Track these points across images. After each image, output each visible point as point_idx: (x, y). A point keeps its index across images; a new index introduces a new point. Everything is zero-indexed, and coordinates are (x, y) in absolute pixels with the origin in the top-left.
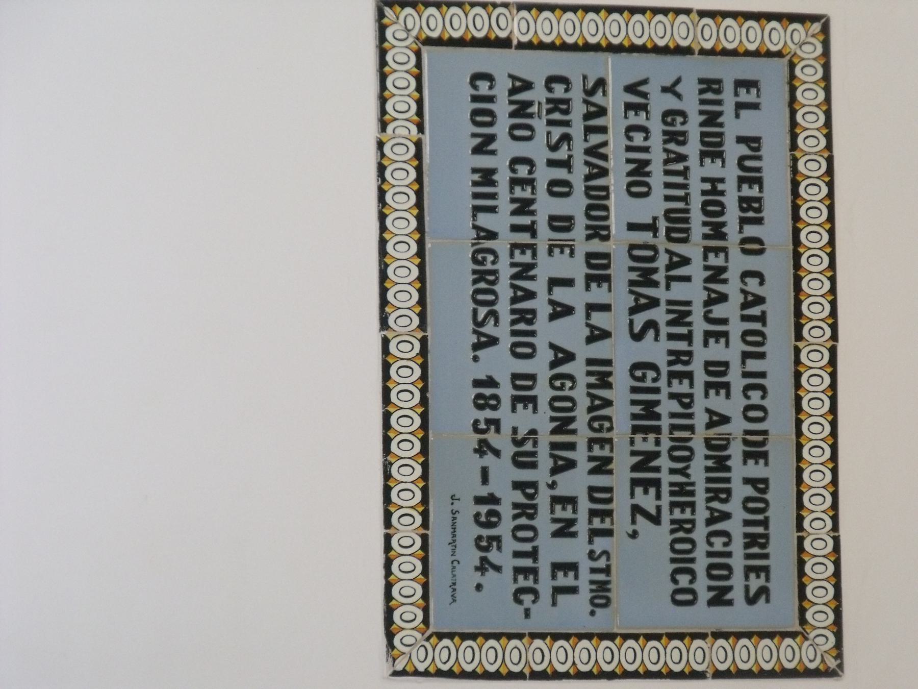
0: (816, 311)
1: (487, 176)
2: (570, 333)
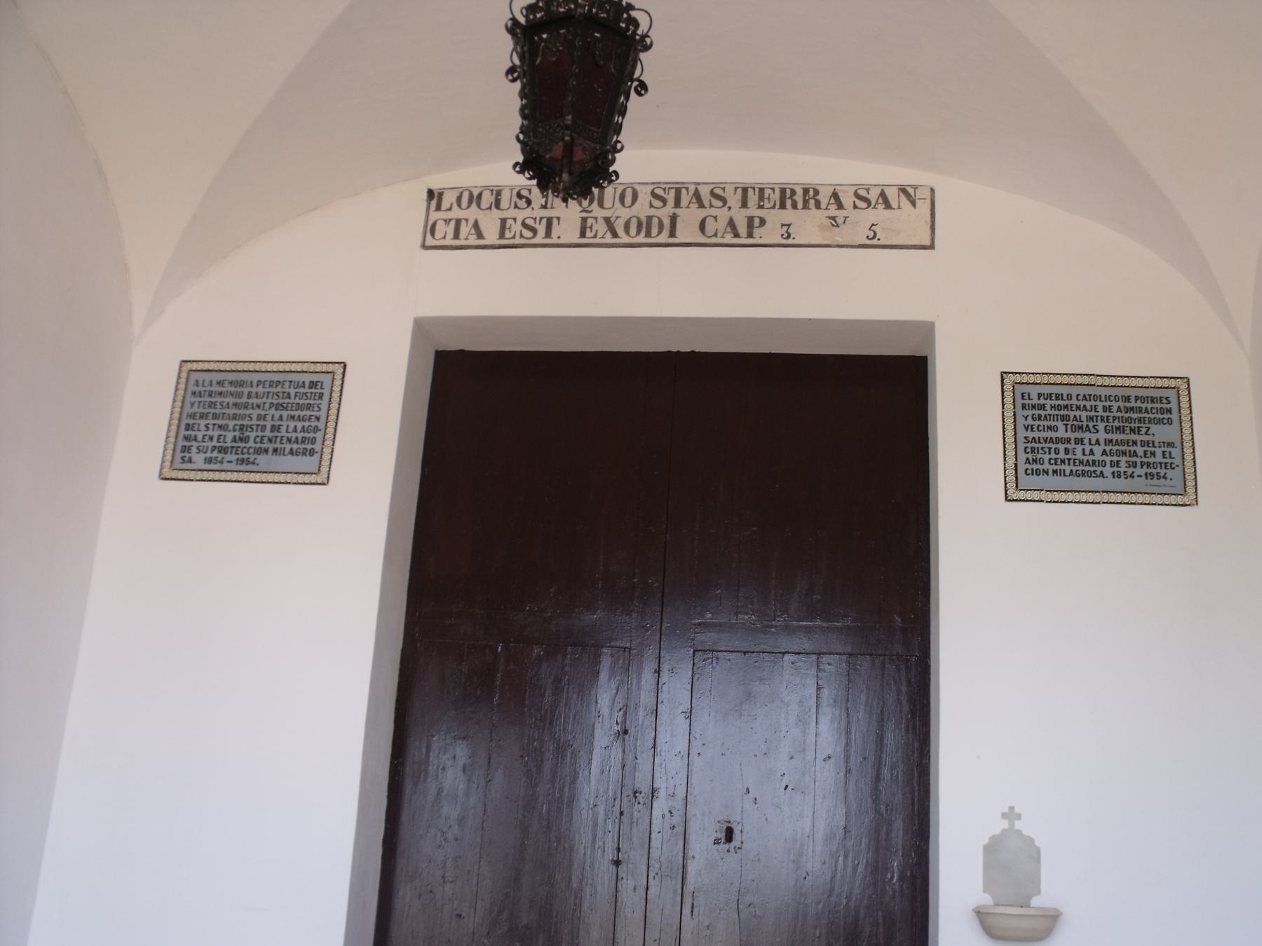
0: (1086, 380)
1: (1055, 472)
2: (1098, 450)
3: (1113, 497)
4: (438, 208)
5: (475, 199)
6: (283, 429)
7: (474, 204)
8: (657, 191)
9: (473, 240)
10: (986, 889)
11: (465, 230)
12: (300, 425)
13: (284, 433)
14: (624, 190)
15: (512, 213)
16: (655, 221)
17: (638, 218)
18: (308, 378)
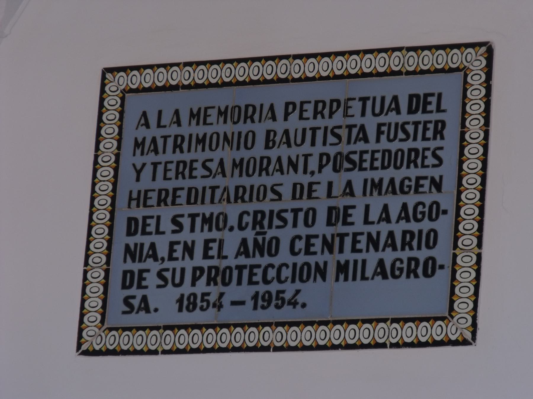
6: (357, 216)
12: (395, 204)
13: (359, 226)
18: (404, 88)
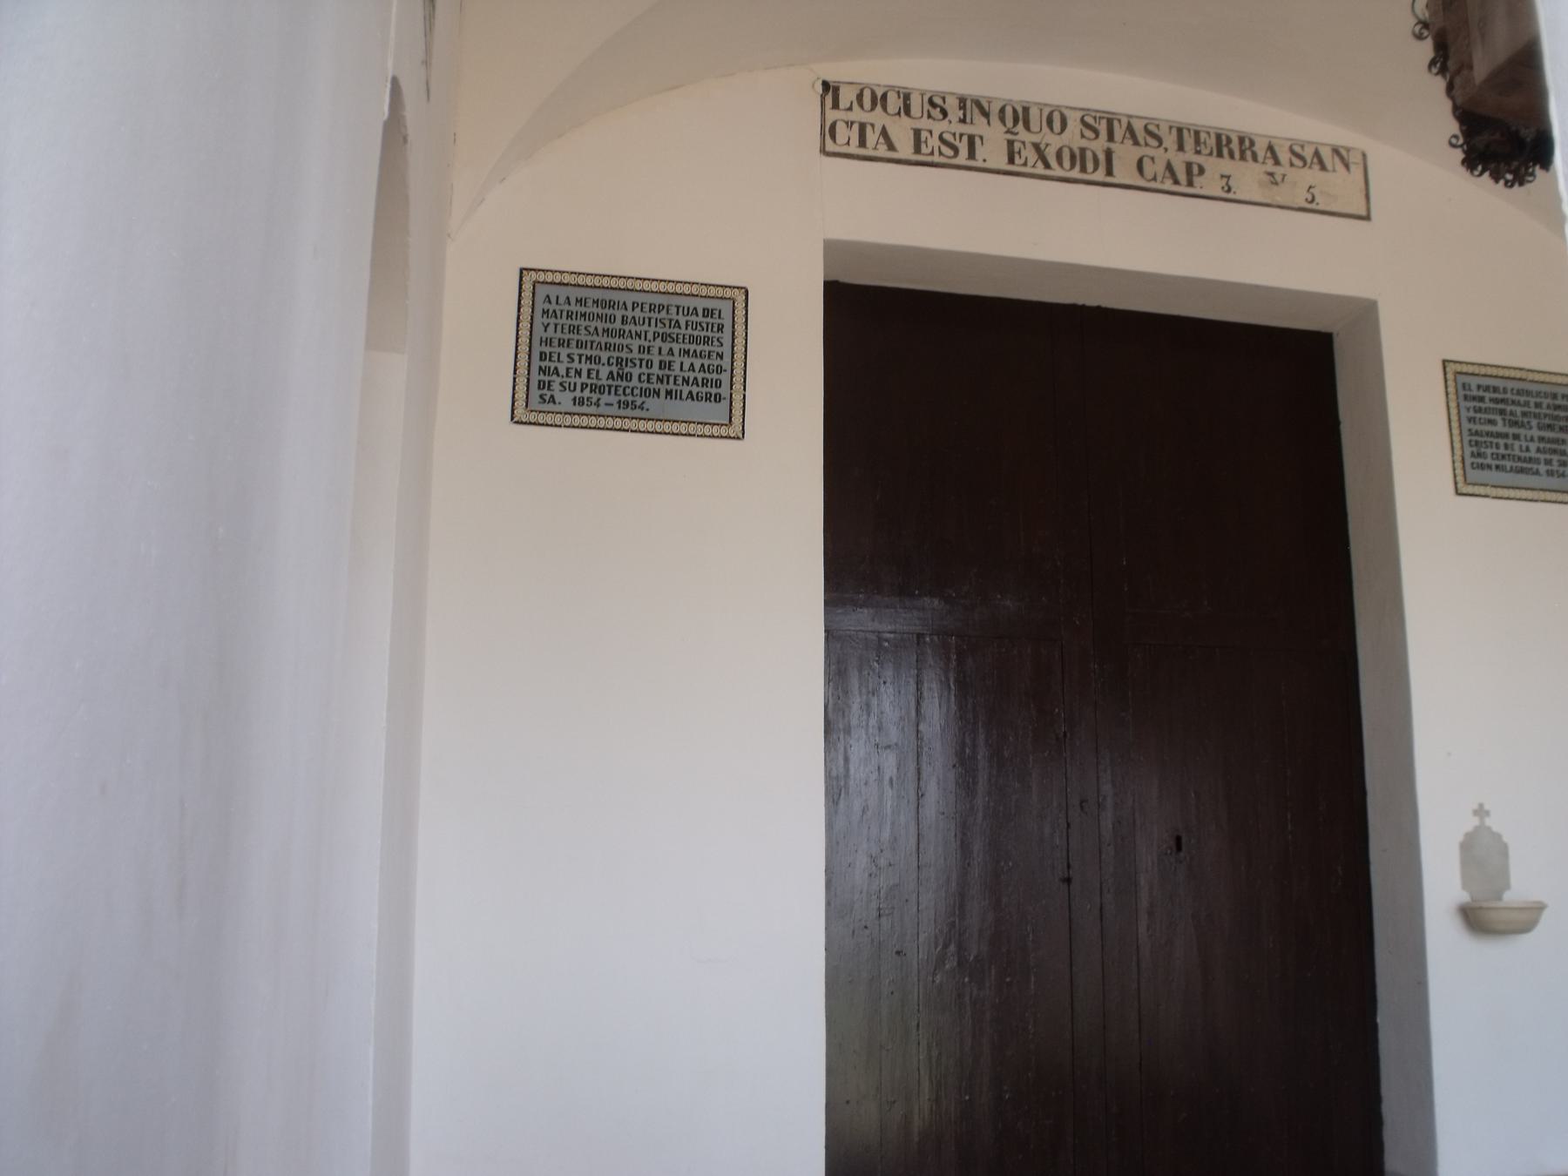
0: (1518, 374)
1: (1497, 467)
2: (1533, 447)
3: (1549, 496)
4: (836, 106)
5: (879, 101)
6: (676, 366)
7: (879, 107)
8: (1087, 119)
9: (882, 151)
10: (1465, 886)
11: (872, 137)
12: (698, 363)
13: (677, 371)
14: (1051, 114)
15: (924, 123)
16: (1089, 155)
17: (1071, 150)
18: (701, 304)
